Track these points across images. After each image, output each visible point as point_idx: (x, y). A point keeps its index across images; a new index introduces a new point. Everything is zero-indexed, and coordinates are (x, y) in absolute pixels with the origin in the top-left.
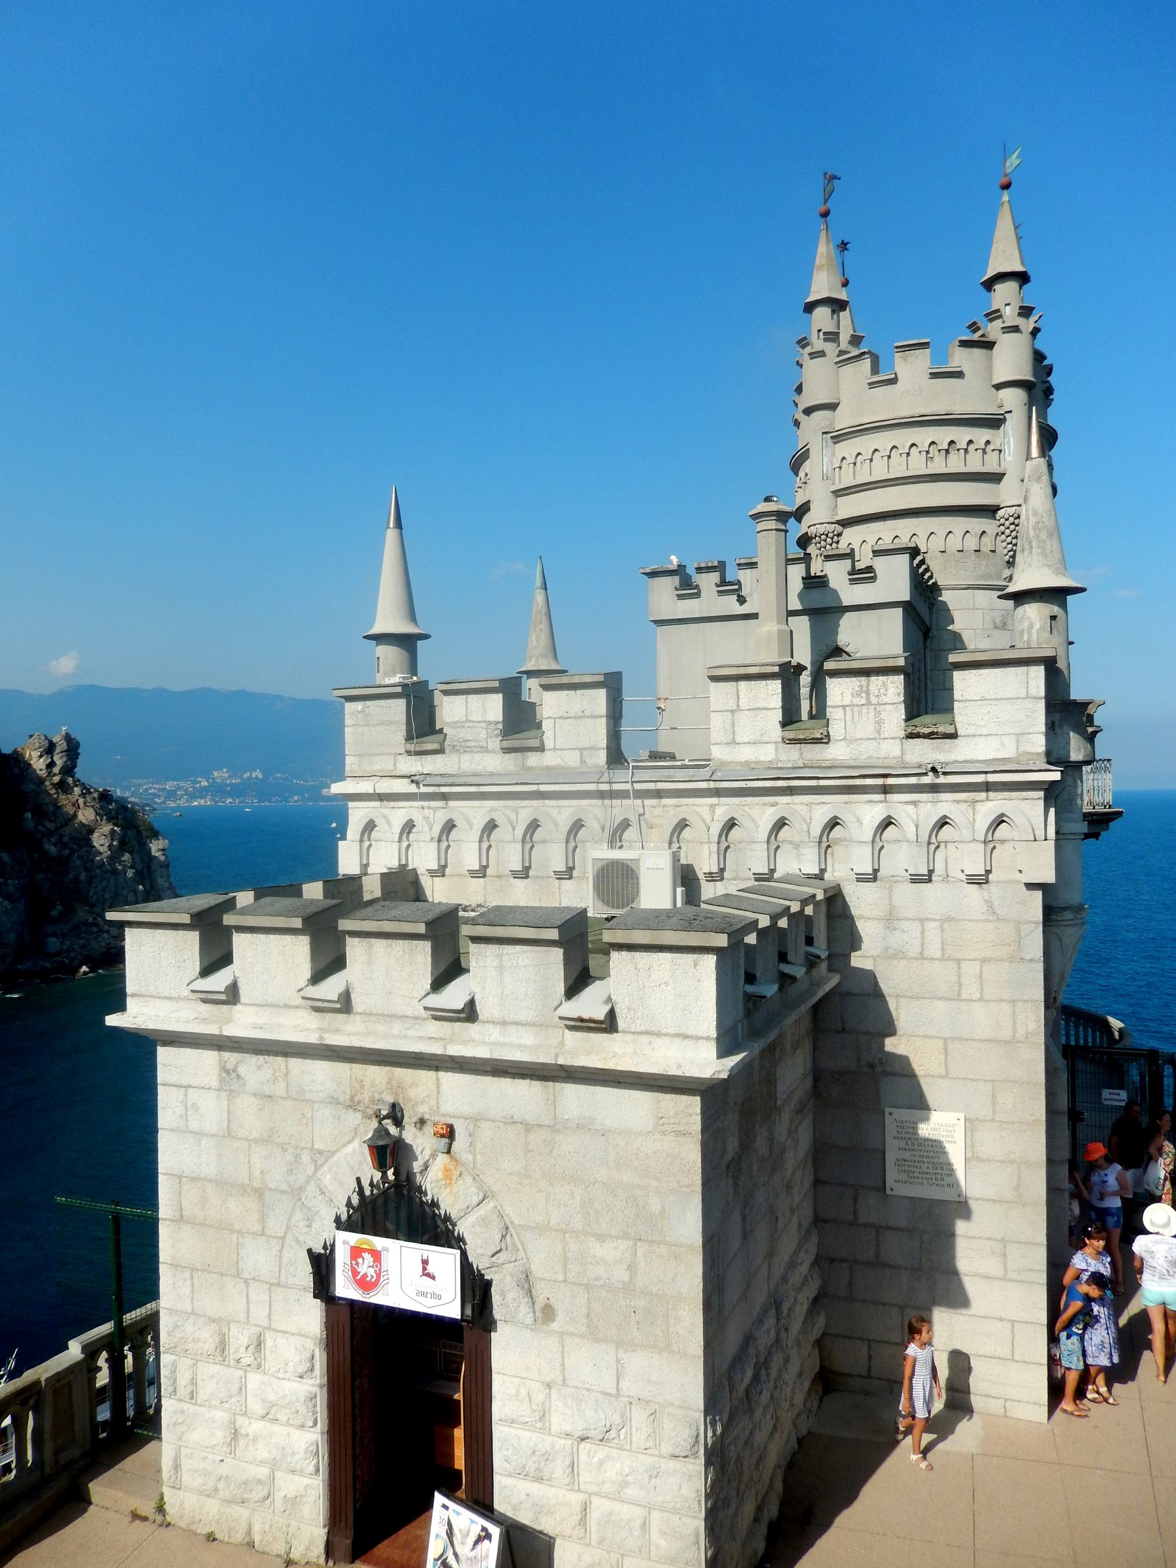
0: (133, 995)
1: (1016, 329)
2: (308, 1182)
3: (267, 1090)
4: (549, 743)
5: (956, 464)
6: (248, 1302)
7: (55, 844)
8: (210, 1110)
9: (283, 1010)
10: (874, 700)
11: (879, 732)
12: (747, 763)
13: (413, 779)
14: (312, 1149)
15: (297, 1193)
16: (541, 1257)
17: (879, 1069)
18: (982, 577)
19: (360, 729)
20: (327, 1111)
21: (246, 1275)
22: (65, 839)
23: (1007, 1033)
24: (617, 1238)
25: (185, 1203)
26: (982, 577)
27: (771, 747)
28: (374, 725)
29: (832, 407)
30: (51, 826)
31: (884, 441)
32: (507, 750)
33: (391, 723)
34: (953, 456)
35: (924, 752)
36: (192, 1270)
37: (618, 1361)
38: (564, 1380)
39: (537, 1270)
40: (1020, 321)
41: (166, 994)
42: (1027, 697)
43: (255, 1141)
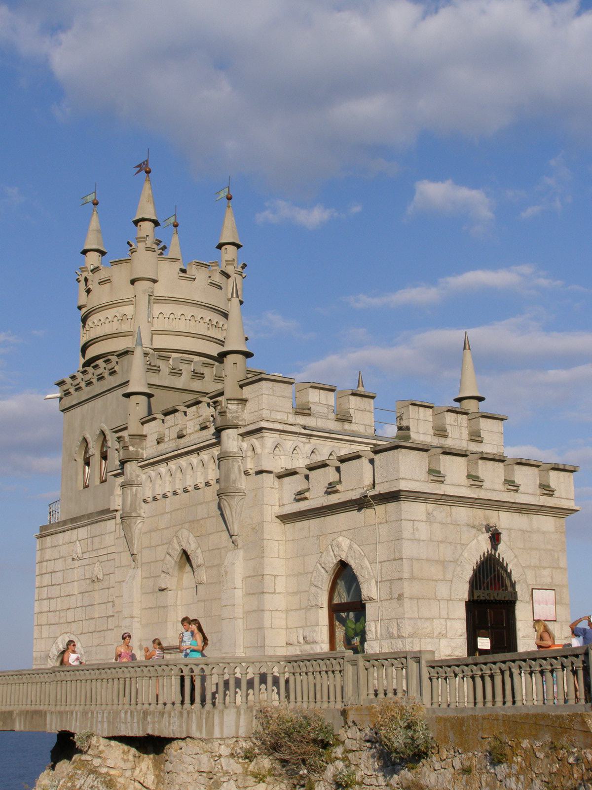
3: (444, 521)
8: (423, 530)
9: (457, 487)
11: (461, 437)
14: (461, 544)
19: (271, 397)
20: (465, 529)
21: (439, 598)
24: (548, 567)
28: (278, 396)
31: (179, 310)
43: (441, 542)
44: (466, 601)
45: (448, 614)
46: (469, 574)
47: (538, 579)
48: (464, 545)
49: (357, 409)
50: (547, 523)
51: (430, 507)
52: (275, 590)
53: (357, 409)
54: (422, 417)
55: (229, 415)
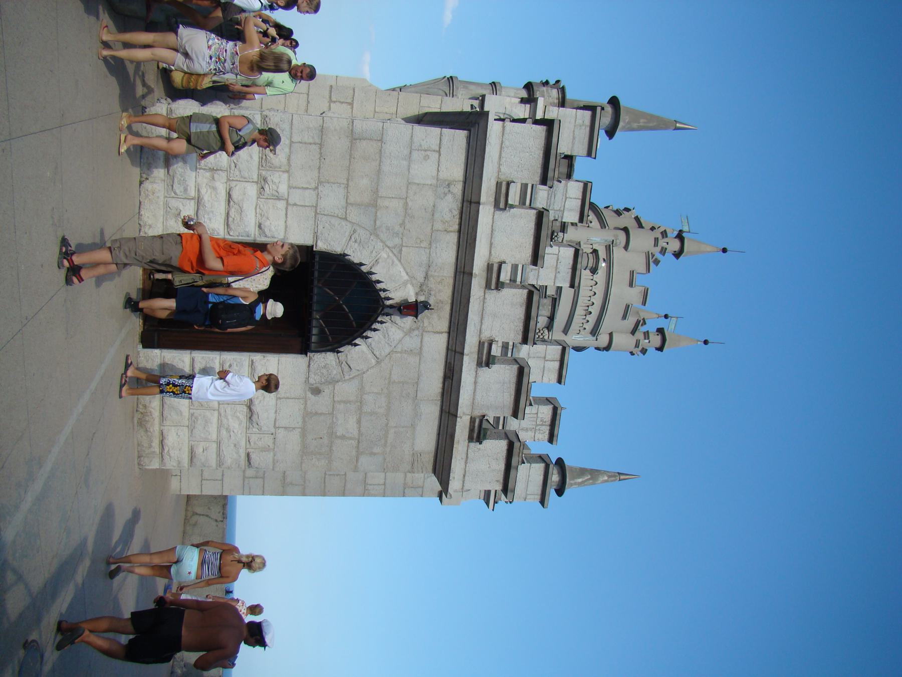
0: (504, 127)
1: (637, 346)
2: (382, 241)
3: (437, 215)
6: (303, 188)
8: (424, 171)
15: (374, 232)
16: (347, 389)
19: (573, 121)
20: (424, 258)
21: (320, 188)
23: (369, 481)
25: (364, 143)
29: (626, 248)
33: (573, 144)
36: (320, 144)
37: (294, 428)
38: (280, 398)
39: (338, 386)
41: (503, 155)
42: (527, 494)
43: (407, 203)
44: (312, 246)
45: (295, 205)
46: (355, 257)
47: (341, 407)
48: (398, 252)
49: (558, 259)
50: (425, 439)
51: (458, 189)
52: (335, 102)
53: (558, 259)
55: (545, 89)
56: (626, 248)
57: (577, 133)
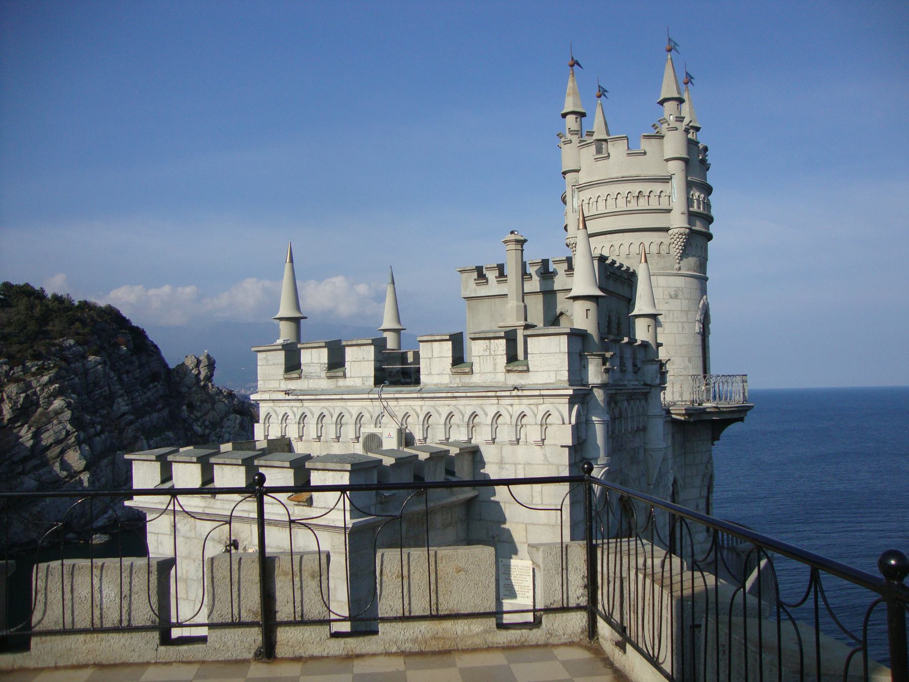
4: (348, 374)
5: (643, 204)
7: (201, 426)
10: (493, 353)
12: (437, 385)
13: (287, 393)
17: (496, 539)
18: (662, 269)
22: (207, 423)
26: (662, 269)
27: (447, 376)
30: (198, 414)
31: (602, 191)
32: (329, 378)
34: (641, 200)
35: (515, 379)
40: (677, 125)
54: (436, 354)
56: (578, 171)
57: (270, 363)
